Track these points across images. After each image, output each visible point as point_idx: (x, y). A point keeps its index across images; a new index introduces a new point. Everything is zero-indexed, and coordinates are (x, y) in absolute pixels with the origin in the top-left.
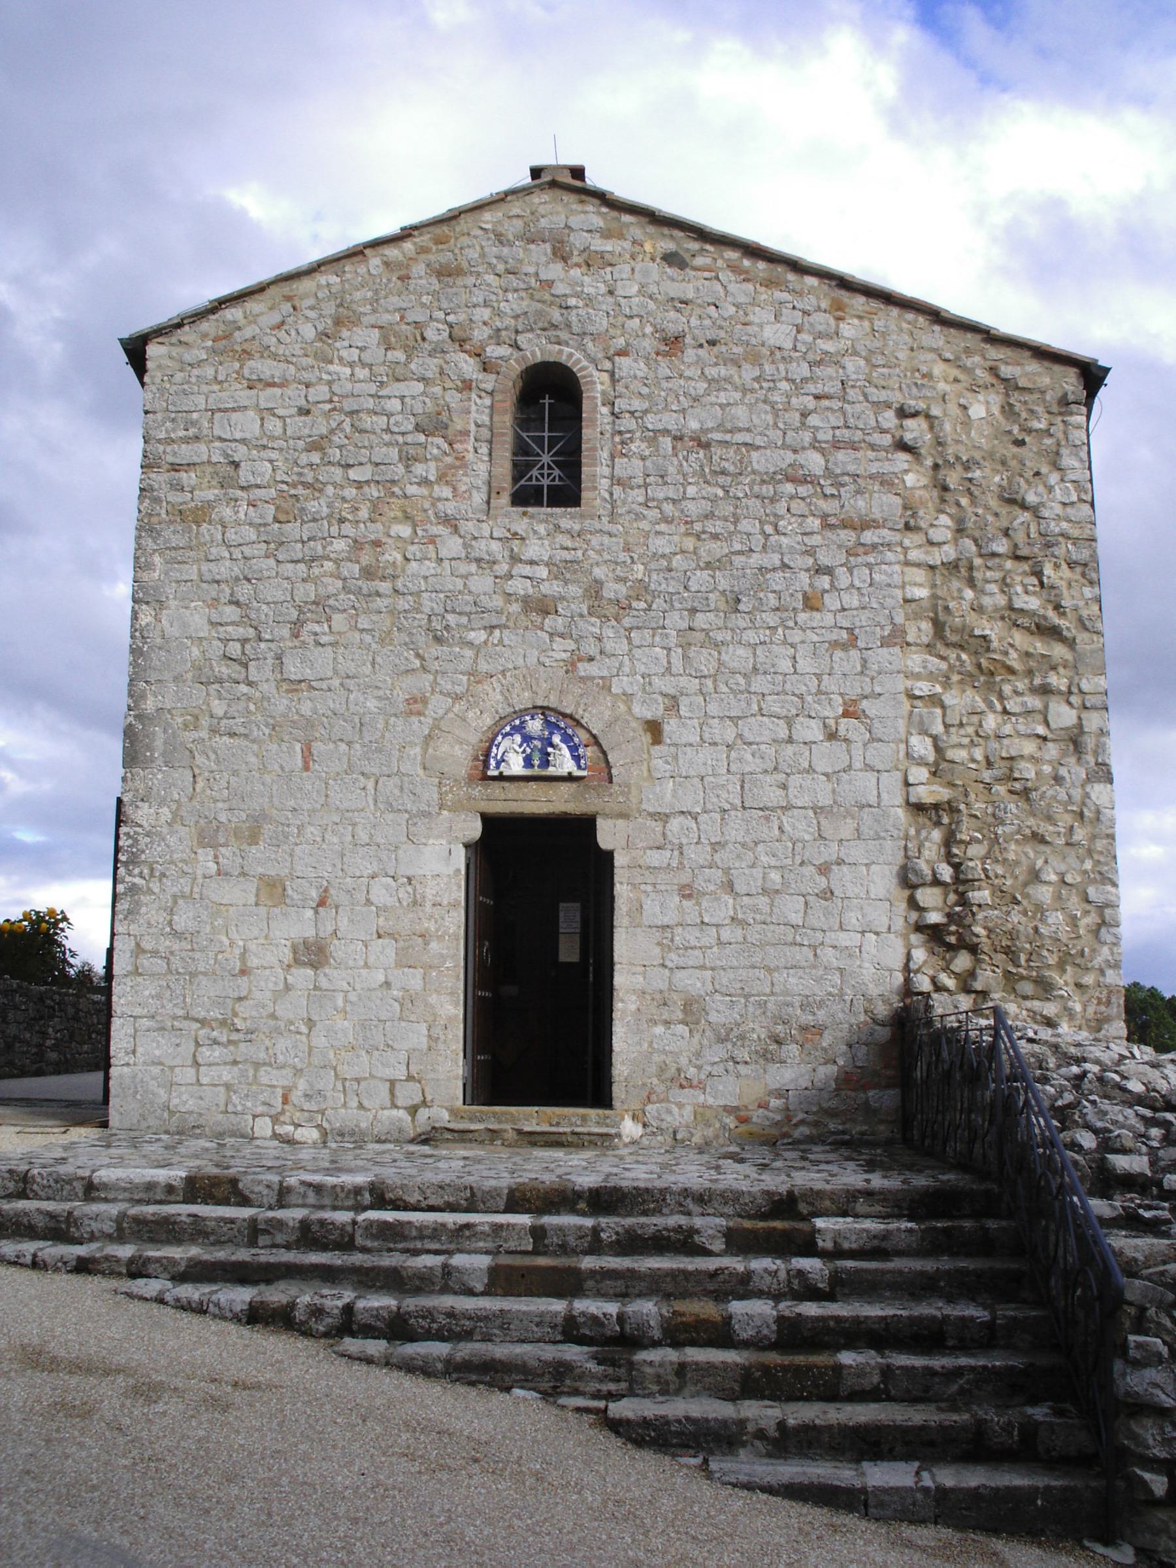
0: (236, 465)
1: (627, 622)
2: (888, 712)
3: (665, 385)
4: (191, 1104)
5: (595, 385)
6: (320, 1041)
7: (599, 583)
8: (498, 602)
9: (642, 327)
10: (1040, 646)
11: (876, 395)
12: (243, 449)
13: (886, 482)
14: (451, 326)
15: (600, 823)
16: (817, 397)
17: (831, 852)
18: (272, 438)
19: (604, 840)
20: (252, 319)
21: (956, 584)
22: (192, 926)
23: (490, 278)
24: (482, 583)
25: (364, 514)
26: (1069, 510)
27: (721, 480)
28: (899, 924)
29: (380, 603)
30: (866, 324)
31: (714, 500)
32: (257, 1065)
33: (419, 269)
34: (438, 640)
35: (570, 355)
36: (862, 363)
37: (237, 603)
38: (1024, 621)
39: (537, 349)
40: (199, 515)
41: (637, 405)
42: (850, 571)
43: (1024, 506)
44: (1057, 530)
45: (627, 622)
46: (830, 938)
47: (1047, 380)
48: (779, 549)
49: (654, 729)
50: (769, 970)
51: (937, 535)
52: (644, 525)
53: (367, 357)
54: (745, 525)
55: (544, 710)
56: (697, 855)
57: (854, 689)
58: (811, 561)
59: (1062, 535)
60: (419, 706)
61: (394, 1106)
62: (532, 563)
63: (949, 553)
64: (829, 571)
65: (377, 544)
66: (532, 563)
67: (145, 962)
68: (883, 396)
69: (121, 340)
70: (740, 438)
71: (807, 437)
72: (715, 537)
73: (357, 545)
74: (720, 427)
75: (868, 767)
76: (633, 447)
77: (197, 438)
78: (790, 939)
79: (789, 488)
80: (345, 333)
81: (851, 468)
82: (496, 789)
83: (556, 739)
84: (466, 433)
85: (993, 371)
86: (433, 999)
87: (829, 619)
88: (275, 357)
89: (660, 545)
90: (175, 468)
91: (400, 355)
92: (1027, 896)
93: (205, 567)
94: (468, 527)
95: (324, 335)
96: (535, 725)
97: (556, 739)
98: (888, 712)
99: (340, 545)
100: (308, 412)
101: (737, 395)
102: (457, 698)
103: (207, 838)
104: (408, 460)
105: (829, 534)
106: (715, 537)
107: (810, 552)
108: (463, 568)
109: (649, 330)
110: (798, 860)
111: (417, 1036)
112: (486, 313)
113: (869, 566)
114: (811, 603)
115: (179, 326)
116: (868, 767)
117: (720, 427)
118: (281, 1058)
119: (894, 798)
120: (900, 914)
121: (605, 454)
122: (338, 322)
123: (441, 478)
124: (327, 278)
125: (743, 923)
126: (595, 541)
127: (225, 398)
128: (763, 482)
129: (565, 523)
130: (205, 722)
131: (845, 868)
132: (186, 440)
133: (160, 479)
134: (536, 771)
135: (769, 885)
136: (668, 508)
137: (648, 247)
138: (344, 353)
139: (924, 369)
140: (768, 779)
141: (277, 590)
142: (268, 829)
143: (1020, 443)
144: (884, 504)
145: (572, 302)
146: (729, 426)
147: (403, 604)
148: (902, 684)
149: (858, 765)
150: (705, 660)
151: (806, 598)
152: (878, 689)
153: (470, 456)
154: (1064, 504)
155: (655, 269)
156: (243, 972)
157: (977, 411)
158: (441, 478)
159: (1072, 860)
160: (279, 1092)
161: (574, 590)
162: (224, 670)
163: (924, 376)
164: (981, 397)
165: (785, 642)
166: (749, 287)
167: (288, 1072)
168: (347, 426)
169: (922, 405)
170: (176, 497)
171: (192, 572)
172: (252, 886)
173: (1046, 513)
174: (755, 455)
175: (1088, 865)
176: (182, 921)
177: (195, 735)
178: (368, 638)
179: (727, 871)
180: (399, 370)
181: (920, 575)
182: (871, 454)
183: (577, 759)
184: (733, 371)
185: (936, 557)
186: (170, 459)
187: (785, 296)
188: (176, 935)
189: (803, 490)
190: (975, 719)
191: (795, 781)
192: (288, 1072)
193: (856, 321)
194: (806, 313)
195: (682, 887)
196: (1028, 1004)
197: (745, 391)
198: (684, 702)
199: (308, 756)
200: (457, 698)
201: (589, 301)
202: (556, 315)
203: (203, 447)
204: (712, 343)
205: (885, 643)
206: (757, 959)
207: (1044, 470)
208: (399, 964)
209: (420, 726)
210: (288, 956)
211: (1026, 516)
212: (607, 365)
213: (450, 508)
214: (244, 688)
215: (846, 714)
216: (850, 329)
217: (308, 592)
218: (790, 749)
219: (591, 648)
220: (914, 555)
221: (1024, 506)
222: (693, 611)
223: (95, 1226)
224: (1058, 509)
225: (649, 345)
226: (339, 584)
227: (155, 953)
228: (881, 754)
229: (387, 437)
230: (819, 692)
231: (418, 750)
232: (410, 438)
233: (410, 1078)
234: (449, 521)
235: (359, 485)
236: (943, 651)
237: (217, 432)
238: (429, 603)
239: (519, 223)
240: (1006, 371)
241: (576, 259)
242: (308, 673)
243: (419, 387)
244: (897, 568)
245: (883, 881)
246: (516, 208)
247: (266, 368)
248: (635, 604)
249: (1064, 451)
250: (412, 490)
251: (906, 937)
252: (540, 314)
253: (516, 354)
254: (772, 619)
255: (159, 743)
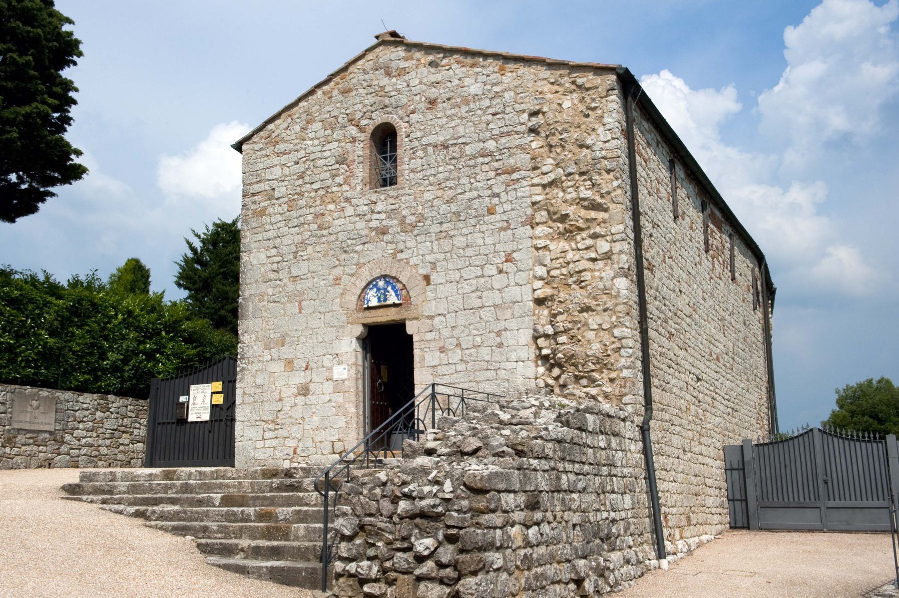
0: (274, 189)
1: (415, 232)
2: (525, 257)
3: (430, 123)
4: (262, 457)
5: (402, 129)
6: (307, 427)
7: (404, 217)
8: (366, 232)
9: (421, 99)
10: (593, 214)
11: (518, 107)
12: (276, 183)
13: (523, 148)
14: (347, 114)
15: (407, 323)
16: (493, 115)
17: (501, 325)
18: (286, 176)
19: (409, 331)
20: (277, 127)
21: (556, 191)
22: (262, 382)
23: (361, 90)
24: (361, 225)
25: (318, 202)
26: (607, 144)
27: (453, 161)
28: (533, 356)
29: (324, 239)
30: (514, 74)
31: (450, 171)
32: (285, 438)
33: (336, 92)
34: (345, 252)
35: (393, 119)
36: (512, 93)
37: (275, 247)
38: (586, 203)
39: (380, 118)
40: (262, 213)
41: (419, 134)
42: (507, 193)
43: (588, 147)
44: (600, 156)
45: (415, 232)
46: (503, 365)
47: (599, 81)
48: (477, 189)
49: (427, 278)
50: (477, 382)
51: (545, 169)
52: (422, 188)
53: (318, 135)
54: (463, 181)
55: (384, 277)
56: (446, 332)
57: (509, 248)
58: (490, 192)
59: (603, 158)
60: (338, 282)
61: (334, 453)
62: (379, 213)
63: (552, 177)
64: (497, 195)
65: (323, 215)
66: (379, 213)
67: (246, 398)
68: (523, 107)
69: (232, 146)
70: (460, 141)
71: (488, 134)
72: (450, 188)
73: (316, 216)
74: (452, 138)
75: (517, 284)
76: (417, 154)
77: (260, 181)
78: (485, 367)
79: (481, 160)
80: (310, 126)
81: (507, 145)
82: (367, 313)
83: (389, 288)
84: (354, 161)
85: (573, 83)
86: (347, 406)
87: (497, 217)
88: (286, 142)
89: (428, 196)
90: (254, 195)
91: (329, 132)
92: (583, 337)
93: (265, 234)
94: (354, 201)
95: (303, 129)
96: (381, 283)
97: (389, 288)
98: (525, 257)
99: (310, 217)
100: (298, 163)
101: (459, 121)
102: (352, 275)
103: (268, 347)
104: (334, 176)
105: (498, 178)
106: (450, 188)
107: (490, 188)
108: (353, 219)
109: (423, 99)
110: (488, 330)
111: (342, 422)
112: (360, 106)
113: (515, 189)
114: (491, 211)
115: (252, 135)
116: (517, 284)
117: (452, 138)
118: (293, 435)
119: (528, 297)
120: (532, 353)
121: (406, 159)
122: (308, 122)
123: (346, 182)
124: (303, 104)
125: (466, 362)
126: (403, 198)
127: (268, 162)
128: (471, 159)
129: (391, 193)
130: (266, 298)
131: (508, 332)
132: (257, 182)
133: (249, 200)
134: (383, 303)
135: (476, 344)
136: (431, 178)
137: (423, 61)
138: (310, 135)
139: (540, 90)
140: (474, 295)
141: (290, 239)
142: (288, 340)
143: (587, 116)
144: (522, 159)
145: (393, 93)
146: (456, 136)
147: (332, 238)
148: (529, 243)
149: (512, 284)
150: (446, 244)
151: (488, 210)
152: (520, 247)
153: (356, 171)
154: (605, 142)
155: (425, 70)
156: (280, 400)
157: (567, 104)
158: (346, 182)
159: (607, 319)
160: (292, 449)
161: (395, 222)
162: (273, 276)
163: (540, 93)
164: (568, 97)
165: (480, 231)
166: (464, 69)
167: (296, 441)
168: (311, 166)
169: (537, 108)
170: (253, 207)
171: (259, 237)
172: (282, 364)
173: (595, 148)
174: (467, 147)
175: (614, 319)
176: (259, 381)
177: (262, 304)
178: (319, 255)
179: (458, 339)
180: (330, 139)
181: (539, 189)
182: (517, 137)
183: (397, 296)
184: (457, 110)
185: (546, 180)
186: (252, 191)
187: (480, 69)
188: (257, 386)
189: (487, 160)
190: (563, 254)
191: (485, 294)
192: (296, 441)
193: (510, 74)
194: (488, 76)
195: (441, 348)
196: (585, 390)
197: (462, 118)
198: (438, 264)
199: (300, 309)
200: (352, 275)
201: (399, 91)
202: (387, 101)
203: (262, 185)
204: (449, 99)
205: (523, 224)
206: (471, 378)
207: (596, 127)
208: (334, 392)
209: (339, 290)
210: (295, 391)
211: (585, 151)
212: (407, 119)
213: (348, 195)
214: (278, 282)
215: (507, 261)
216: (508, 78)
217: (298, 238)
218: (483, 280)
219: (401, 246)
220: (536, 180)
221: (588, 147)
222: (441, 223)
223: (121, 489)
224: (601, 145)
225: (423, 106)
226: (309, 233)
227: (250, 395)
228: (522, 277)
229: (325, 168)
230: (495, 252)
231: (339, 300)
232: (333, 167)
233: (339, 440)
234: (347, 200)
235: (316, 191)
236: (551, 223)
237: (267, 177)
238: (341, 237)
239: (371, 62)
240: (580, 81)
241: (394, 74)
242: (300, 273)
243: (336, 144)
244: (528, 188)
245: (525, 336)
246: (370, 56)
247: (282, 147)
248: (419, 224)
249: (606, 115)
250: (335, 189)
251: (536, 362)
252: (380, 102)
253: (372, 122)
254: (473, 222)
255: (250, 309)
